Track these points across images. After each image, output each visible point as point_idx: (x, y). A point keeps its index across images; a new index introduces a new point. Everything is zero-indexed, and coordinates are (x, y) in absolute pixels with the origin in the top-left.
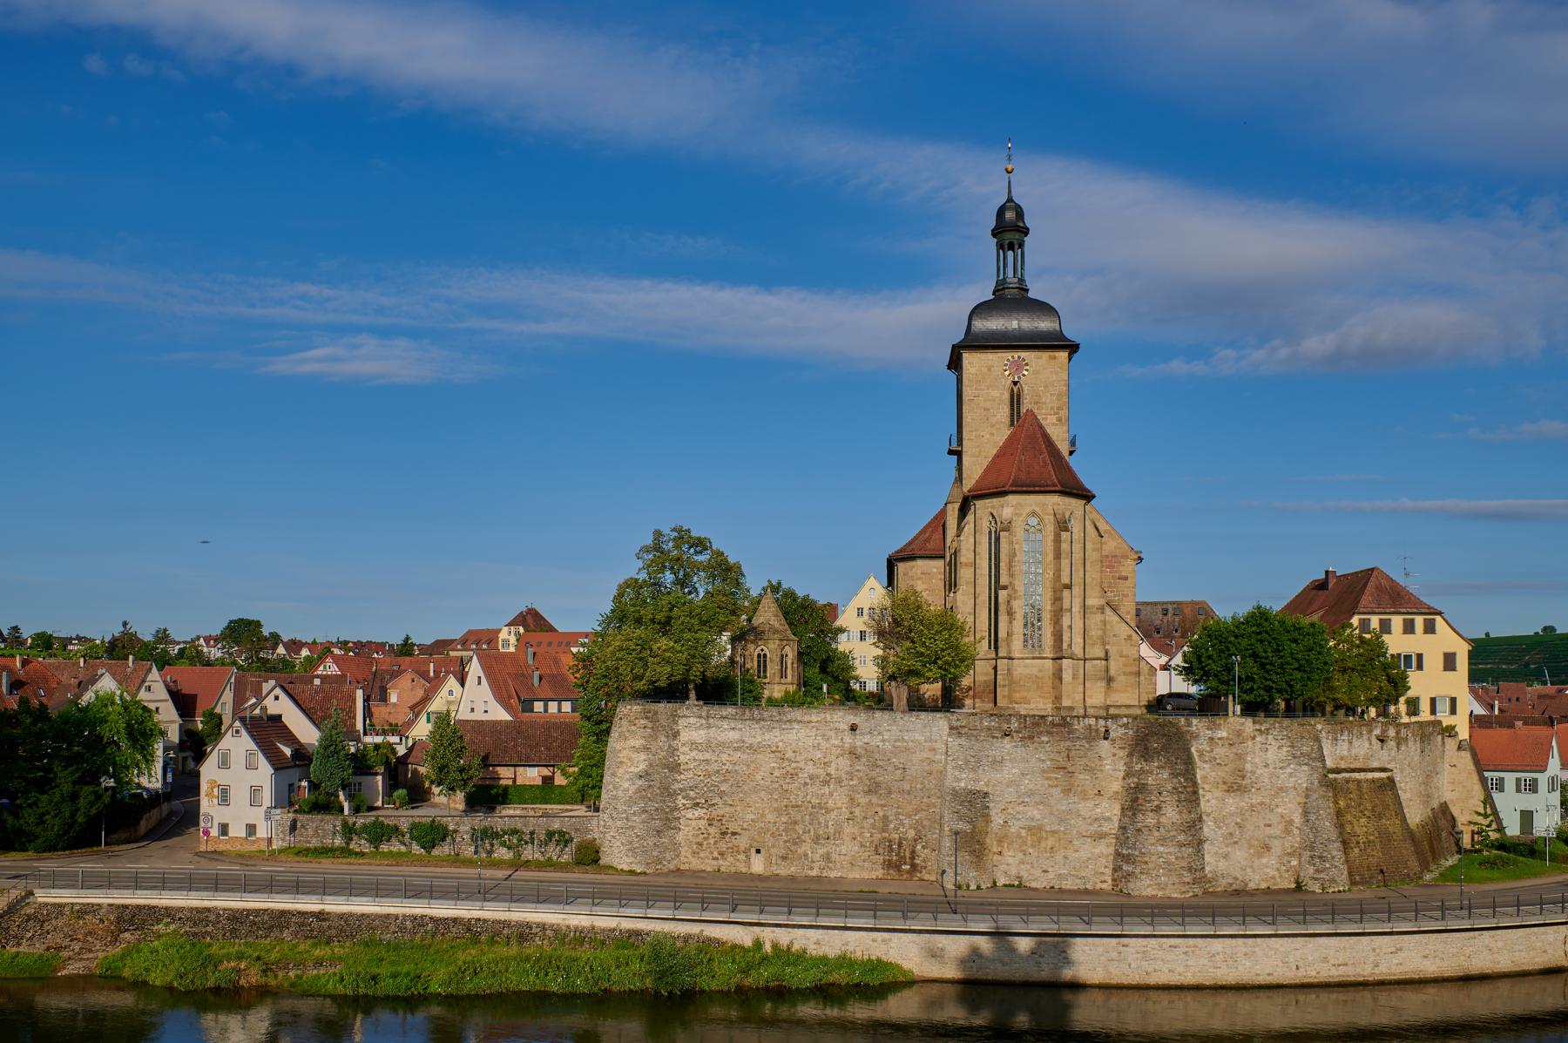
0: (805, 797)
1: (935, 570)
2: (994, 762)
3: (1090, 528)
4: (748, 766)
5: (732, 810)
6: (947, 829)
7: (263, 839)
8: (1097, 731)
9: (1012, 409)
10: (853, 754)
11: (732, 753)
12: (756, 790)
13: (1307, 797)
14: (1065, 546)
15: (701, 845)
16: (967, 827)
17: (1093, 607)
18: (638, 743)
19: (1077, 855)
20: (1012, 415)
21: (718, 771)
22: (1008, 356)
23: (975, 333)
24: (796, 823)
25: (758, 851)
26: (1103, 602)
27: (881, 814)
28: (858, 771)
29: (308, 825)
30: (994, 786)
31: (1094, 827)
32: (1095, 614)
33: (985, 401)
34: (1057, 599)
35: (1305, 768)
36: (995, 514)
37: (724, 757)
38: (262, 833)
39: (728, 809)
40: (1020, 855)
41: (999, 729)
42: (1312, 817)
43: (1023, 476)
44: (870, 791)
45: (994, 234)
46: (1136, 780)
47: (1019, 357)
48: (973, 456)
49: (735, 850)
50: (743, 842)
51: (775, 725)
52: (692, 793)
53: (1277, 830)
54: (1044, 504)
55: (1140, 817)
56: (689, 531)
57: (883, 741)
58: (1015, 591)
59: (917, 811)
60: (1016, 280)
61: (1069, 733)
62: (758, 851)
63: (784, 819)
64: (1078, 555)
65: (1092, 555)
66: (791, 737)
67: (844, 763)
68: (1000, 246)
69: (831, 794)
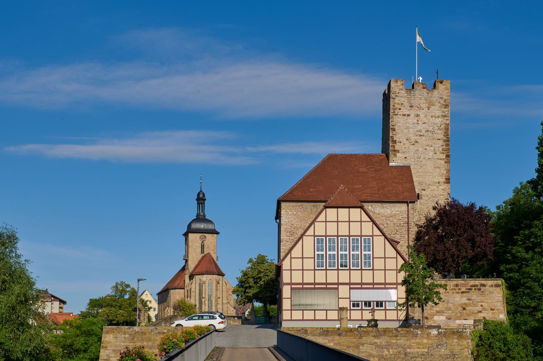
1: (181, 292)
3: (224, 283)
9: (202, 249)
14: (218, 288)
17: (224, 303)
20: (202, 250)
22: (201, 234)
23: (192, 229)
26: (227, 302)
32: (225, 304)
33: (195, 246)
34: (216, 301)
36: (201, 279)
43: (208, 270)
45: (197, 200)
47: (204, 235)
48: (191, 261)
54: (213, 277)
56: (125, 282)
58: (206, 299)
60: (203, 214)
64: (221, 290)
65: (225, 290)
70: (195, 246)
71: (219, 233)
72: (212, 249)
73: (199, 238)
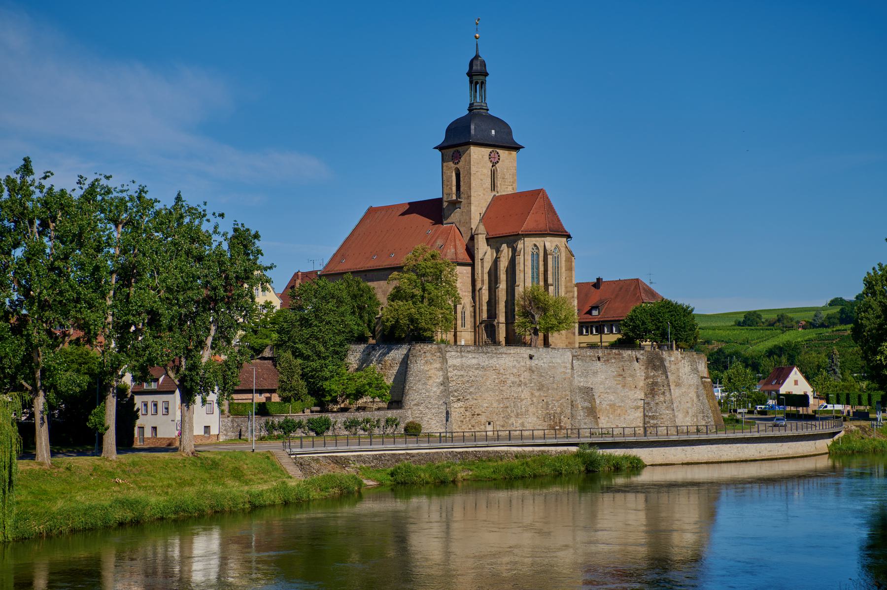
0: (510, 393)
2: (594, 373)
4: (483, 378)
5: (476, 402)
6: (580, 406)
7: (214, 435)
8: (632, 357)
10: (531, 370)
11: (474, 371)
12: (487, 390)
13: (698, 389)
15: (463, 422)
16: (589, 405)
18: (438, 365)
19: (629, 417)
21: (468, 381)
22: (490, 150)
24: (507, 407)
25: (489, 424)
27: (545, 400)
28: (533, 379)
29: (242, 424)
30: (595, 384)
31: (635, 404)
33: (481, 175)
35: (696, 375)
36: (538, 245)
37: (471, 373)
38: (214, 431)
39: (475, 401)
40: (607, 419)
41: (594, 356)
42: (701, 398)
44: (540, 389)
46: (652, 380)
48: (475, 206)
49: (479, 423)
50: (483, 418)
51: (494, 355)
52: (456, 393)
53: (689, 405)
55: (657, 397)
57: (544, 363)
59: (561, 398)
61: (622, 358)
62: (489, 424)
63: (502, 405)
66: (502, 361)
67: (527, 374)
68: (471, 82)
69: (522, 392)
70: (481, 175)
71: (523, 147)
72: (509, 180)
73: (488, 158)
